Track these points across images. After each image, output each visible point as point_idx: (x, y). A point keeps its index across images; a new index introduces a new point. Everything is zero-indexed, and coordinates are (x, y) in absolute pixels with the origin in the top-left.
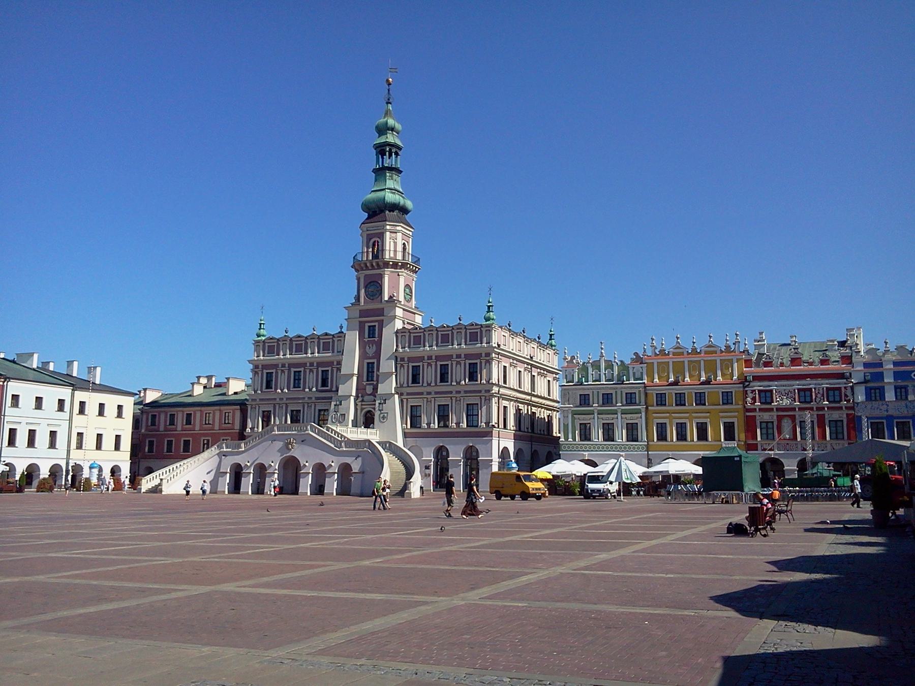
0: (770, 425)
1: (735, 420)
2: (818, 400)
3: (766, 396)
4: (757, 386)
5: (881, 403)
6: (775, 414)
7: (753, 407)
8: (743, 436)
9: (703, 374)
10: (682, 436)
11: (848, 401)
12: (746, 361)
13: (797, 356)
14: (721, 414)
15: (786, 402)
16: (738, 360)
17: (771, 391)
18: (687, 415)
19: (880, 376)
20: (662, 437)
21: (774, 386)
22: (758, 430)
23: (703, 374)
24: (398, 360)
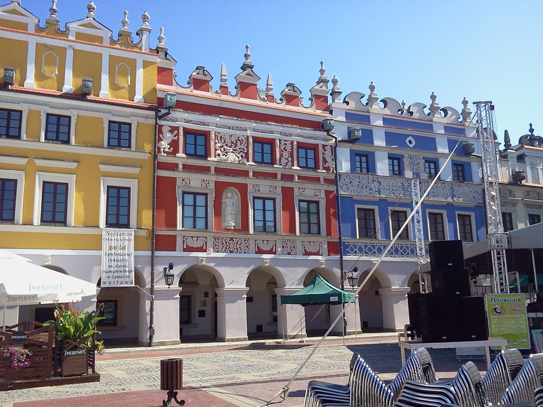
0: (200, 200)
1: (133, 185)
2: (284, 161)
4: (182, 119)
5: (371, 178)
6: (212, 178)
7: (171, 160)
8: (147, 217)
9: (69, 74)
11: (328, 169)
12: (161, 70)
13: (249, 80)
14: (104, 168)
15: (232, 157)
16: (146, 64)
17: (206, 135)
18: (23, 161)
19: (368, 136)
21: (213, 124)
22: (179, 209)
23: (69, 74)
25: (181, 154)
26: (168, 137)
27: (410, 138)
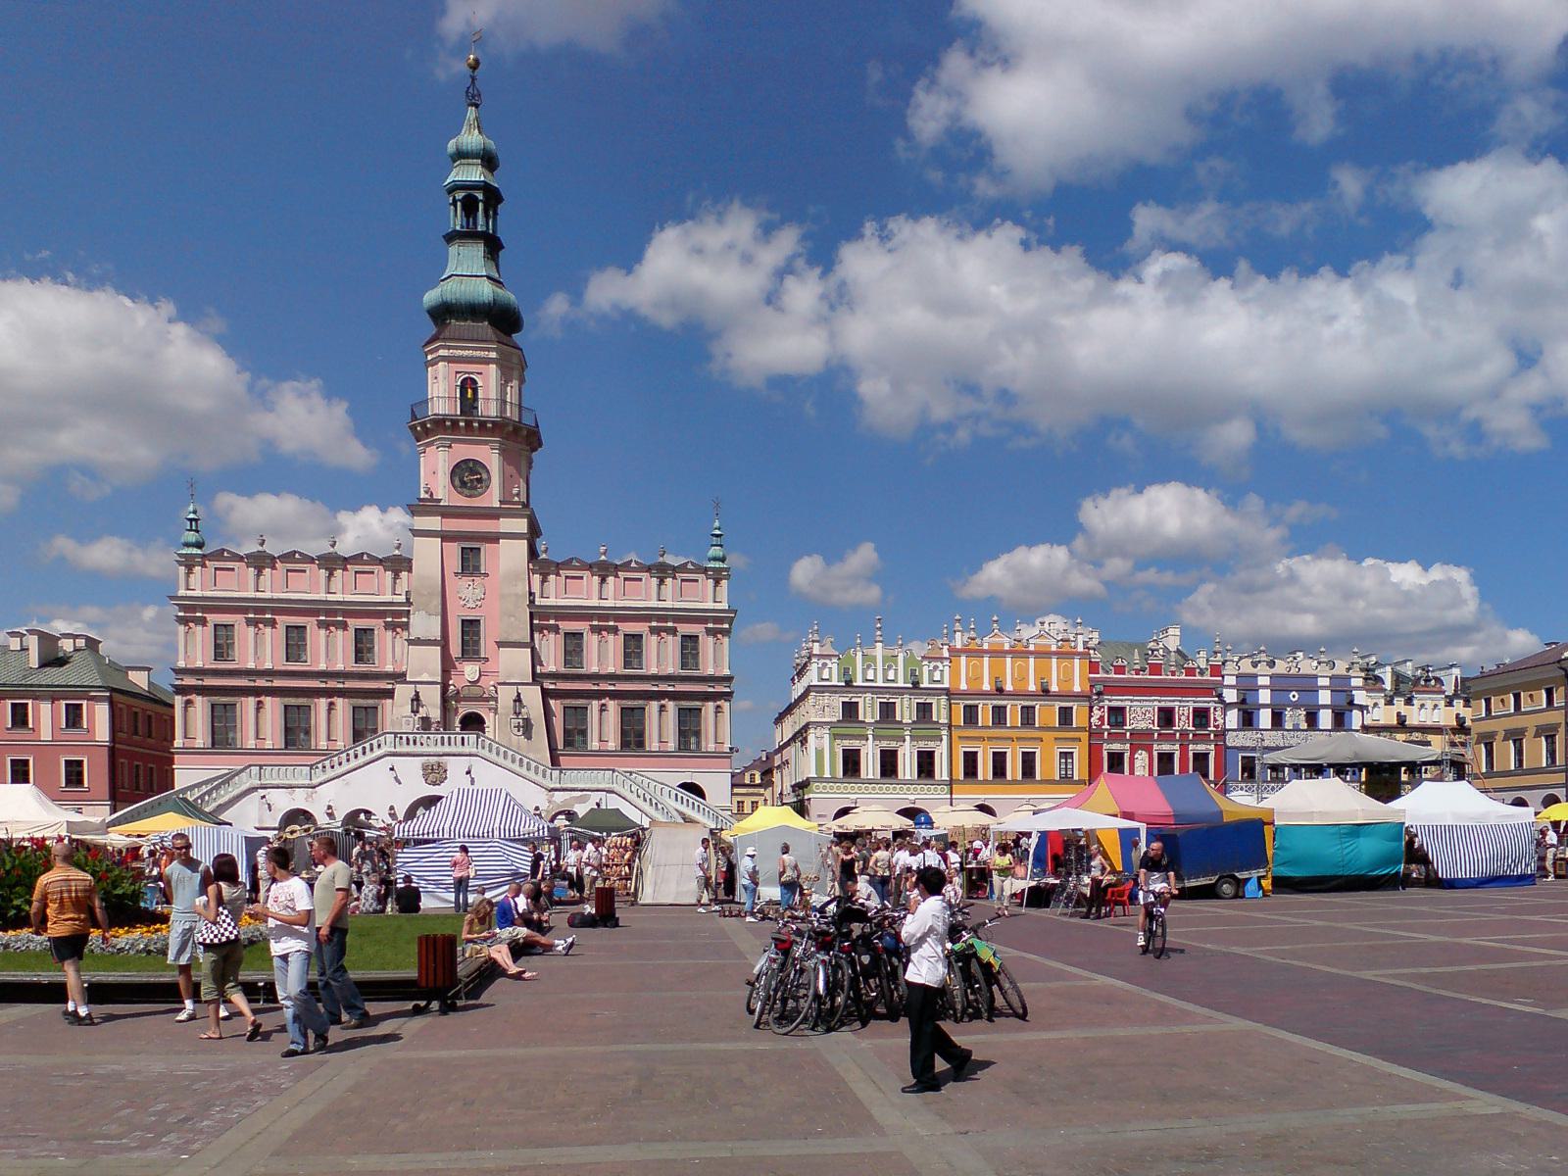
3: (1117, 713)
10: (999, 770)
11: (1216, 726)
15: (1142, 725)
17: (1122, 709)
20: (971, 769)
24: (541, 619)
25: (1106, 726)
26: (1097, 713)
27: (1294, 693)
